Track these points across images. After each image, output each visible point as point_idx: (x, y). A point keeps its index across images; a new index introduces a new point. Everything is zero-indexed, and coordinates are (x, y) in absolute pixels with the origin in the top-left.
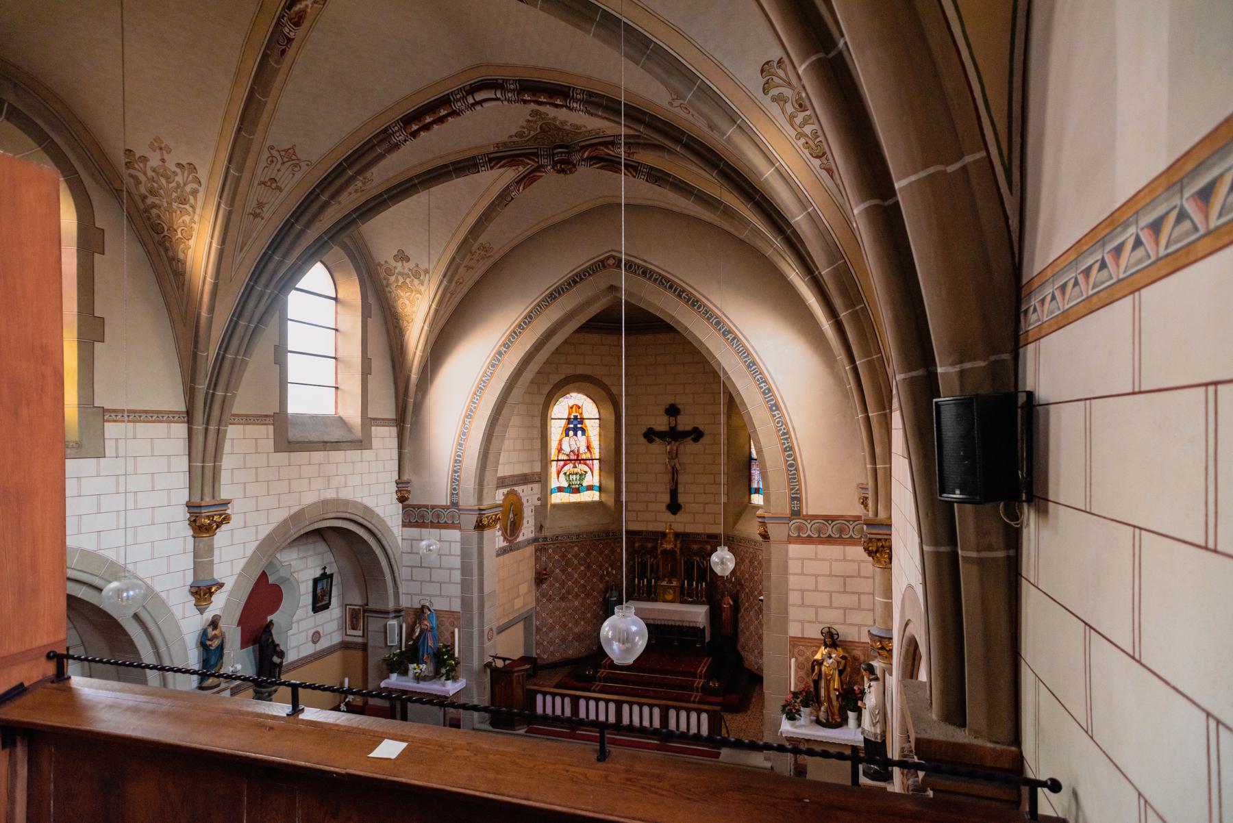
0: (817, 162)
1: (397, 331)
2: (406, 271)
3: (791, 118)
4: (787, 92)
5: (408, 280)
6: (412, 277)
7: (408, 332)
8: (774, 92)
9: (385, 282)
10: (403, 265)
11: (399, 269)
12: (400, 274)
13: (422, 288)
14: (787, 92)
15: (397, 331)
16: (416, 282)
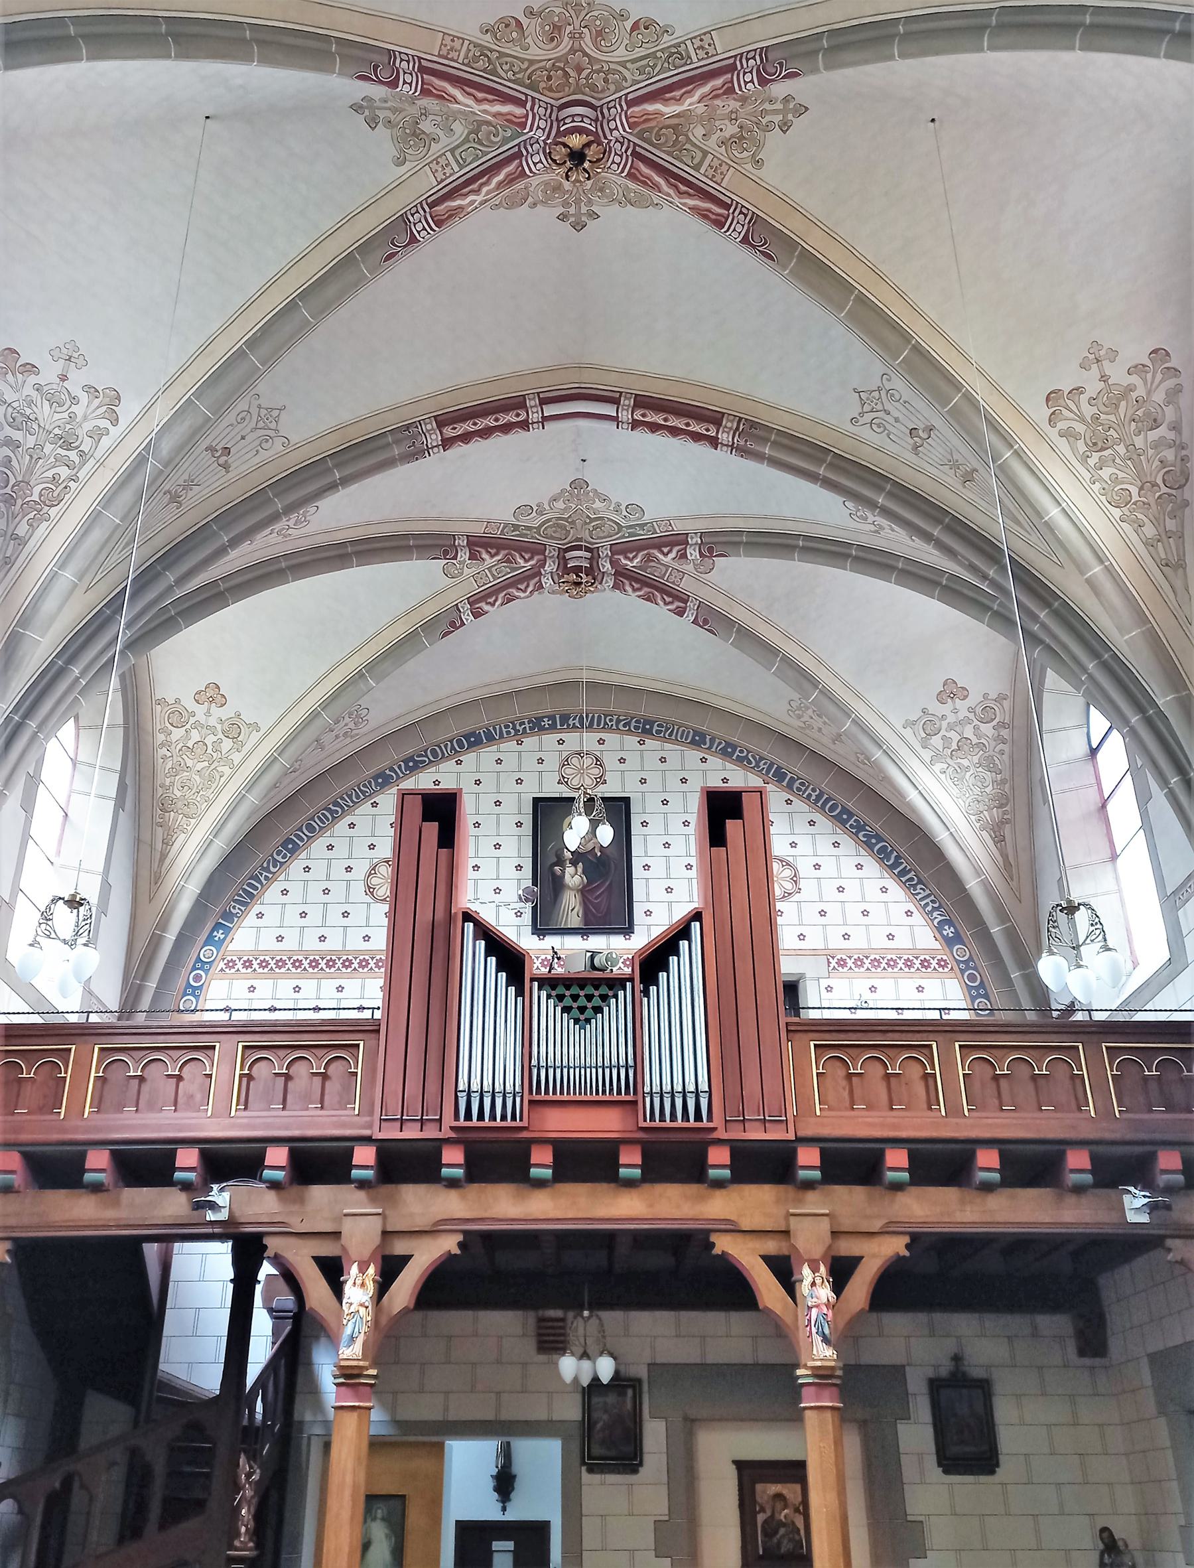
0: (1117, 513)
1: (160, 830)
2: (212, 721)
3: (1084, 459)
4: (1080, 428)
5: (210, 740)
6: (221, 736)
7: (182, 836)
8: (1062, 425)
9: (161, 737)
10: (209, 709)
11: (200, 716)
12: (197, 725)
13: (237, 758)
14: (1080, 428)
15: (160, 830)
16: (227, 744)
